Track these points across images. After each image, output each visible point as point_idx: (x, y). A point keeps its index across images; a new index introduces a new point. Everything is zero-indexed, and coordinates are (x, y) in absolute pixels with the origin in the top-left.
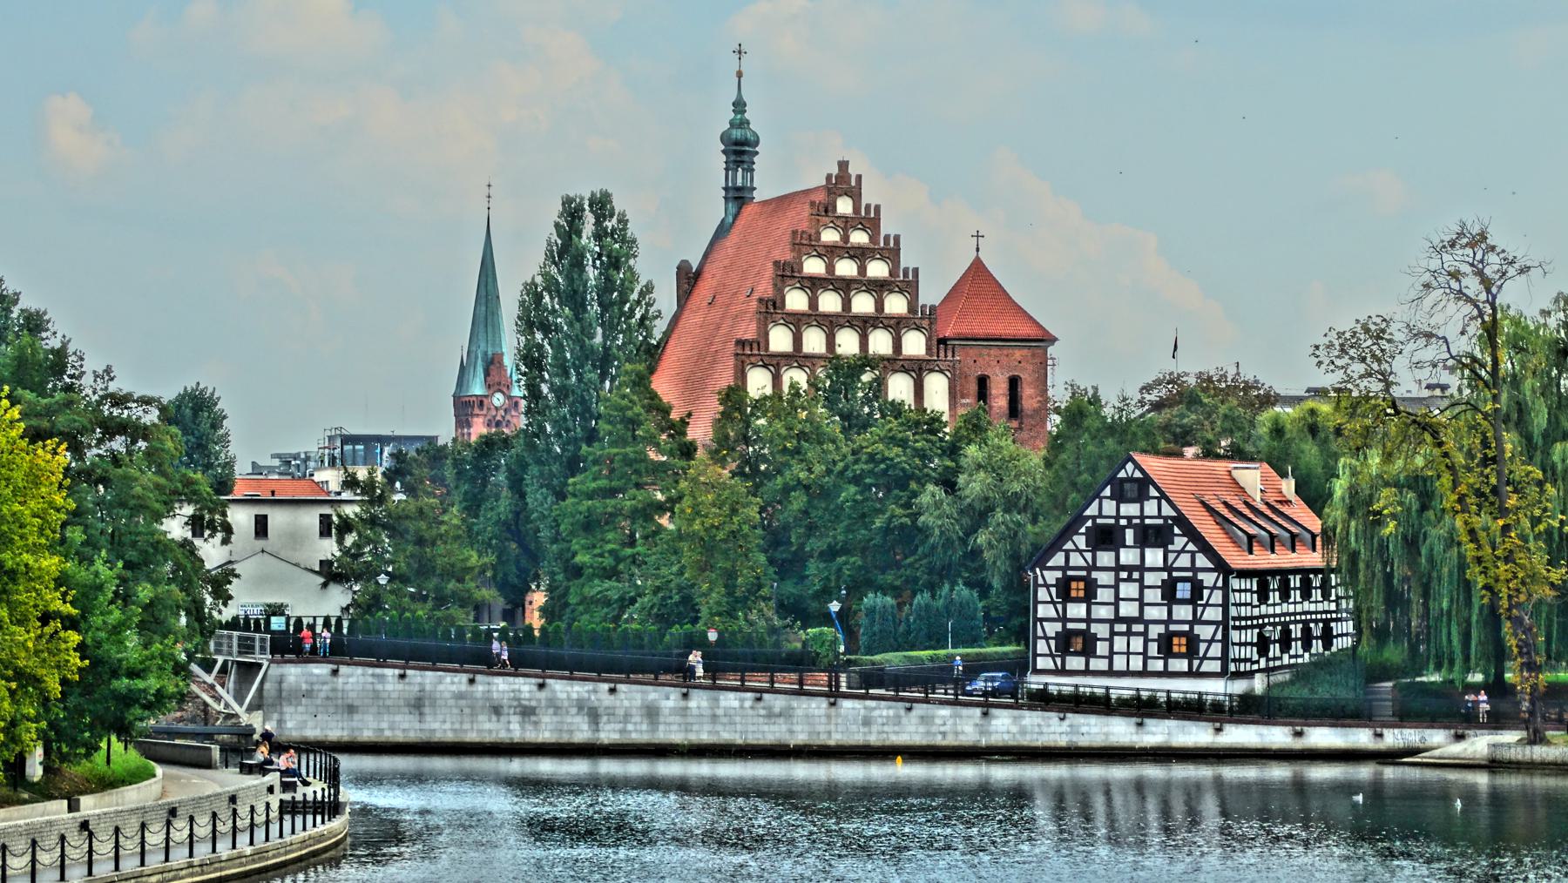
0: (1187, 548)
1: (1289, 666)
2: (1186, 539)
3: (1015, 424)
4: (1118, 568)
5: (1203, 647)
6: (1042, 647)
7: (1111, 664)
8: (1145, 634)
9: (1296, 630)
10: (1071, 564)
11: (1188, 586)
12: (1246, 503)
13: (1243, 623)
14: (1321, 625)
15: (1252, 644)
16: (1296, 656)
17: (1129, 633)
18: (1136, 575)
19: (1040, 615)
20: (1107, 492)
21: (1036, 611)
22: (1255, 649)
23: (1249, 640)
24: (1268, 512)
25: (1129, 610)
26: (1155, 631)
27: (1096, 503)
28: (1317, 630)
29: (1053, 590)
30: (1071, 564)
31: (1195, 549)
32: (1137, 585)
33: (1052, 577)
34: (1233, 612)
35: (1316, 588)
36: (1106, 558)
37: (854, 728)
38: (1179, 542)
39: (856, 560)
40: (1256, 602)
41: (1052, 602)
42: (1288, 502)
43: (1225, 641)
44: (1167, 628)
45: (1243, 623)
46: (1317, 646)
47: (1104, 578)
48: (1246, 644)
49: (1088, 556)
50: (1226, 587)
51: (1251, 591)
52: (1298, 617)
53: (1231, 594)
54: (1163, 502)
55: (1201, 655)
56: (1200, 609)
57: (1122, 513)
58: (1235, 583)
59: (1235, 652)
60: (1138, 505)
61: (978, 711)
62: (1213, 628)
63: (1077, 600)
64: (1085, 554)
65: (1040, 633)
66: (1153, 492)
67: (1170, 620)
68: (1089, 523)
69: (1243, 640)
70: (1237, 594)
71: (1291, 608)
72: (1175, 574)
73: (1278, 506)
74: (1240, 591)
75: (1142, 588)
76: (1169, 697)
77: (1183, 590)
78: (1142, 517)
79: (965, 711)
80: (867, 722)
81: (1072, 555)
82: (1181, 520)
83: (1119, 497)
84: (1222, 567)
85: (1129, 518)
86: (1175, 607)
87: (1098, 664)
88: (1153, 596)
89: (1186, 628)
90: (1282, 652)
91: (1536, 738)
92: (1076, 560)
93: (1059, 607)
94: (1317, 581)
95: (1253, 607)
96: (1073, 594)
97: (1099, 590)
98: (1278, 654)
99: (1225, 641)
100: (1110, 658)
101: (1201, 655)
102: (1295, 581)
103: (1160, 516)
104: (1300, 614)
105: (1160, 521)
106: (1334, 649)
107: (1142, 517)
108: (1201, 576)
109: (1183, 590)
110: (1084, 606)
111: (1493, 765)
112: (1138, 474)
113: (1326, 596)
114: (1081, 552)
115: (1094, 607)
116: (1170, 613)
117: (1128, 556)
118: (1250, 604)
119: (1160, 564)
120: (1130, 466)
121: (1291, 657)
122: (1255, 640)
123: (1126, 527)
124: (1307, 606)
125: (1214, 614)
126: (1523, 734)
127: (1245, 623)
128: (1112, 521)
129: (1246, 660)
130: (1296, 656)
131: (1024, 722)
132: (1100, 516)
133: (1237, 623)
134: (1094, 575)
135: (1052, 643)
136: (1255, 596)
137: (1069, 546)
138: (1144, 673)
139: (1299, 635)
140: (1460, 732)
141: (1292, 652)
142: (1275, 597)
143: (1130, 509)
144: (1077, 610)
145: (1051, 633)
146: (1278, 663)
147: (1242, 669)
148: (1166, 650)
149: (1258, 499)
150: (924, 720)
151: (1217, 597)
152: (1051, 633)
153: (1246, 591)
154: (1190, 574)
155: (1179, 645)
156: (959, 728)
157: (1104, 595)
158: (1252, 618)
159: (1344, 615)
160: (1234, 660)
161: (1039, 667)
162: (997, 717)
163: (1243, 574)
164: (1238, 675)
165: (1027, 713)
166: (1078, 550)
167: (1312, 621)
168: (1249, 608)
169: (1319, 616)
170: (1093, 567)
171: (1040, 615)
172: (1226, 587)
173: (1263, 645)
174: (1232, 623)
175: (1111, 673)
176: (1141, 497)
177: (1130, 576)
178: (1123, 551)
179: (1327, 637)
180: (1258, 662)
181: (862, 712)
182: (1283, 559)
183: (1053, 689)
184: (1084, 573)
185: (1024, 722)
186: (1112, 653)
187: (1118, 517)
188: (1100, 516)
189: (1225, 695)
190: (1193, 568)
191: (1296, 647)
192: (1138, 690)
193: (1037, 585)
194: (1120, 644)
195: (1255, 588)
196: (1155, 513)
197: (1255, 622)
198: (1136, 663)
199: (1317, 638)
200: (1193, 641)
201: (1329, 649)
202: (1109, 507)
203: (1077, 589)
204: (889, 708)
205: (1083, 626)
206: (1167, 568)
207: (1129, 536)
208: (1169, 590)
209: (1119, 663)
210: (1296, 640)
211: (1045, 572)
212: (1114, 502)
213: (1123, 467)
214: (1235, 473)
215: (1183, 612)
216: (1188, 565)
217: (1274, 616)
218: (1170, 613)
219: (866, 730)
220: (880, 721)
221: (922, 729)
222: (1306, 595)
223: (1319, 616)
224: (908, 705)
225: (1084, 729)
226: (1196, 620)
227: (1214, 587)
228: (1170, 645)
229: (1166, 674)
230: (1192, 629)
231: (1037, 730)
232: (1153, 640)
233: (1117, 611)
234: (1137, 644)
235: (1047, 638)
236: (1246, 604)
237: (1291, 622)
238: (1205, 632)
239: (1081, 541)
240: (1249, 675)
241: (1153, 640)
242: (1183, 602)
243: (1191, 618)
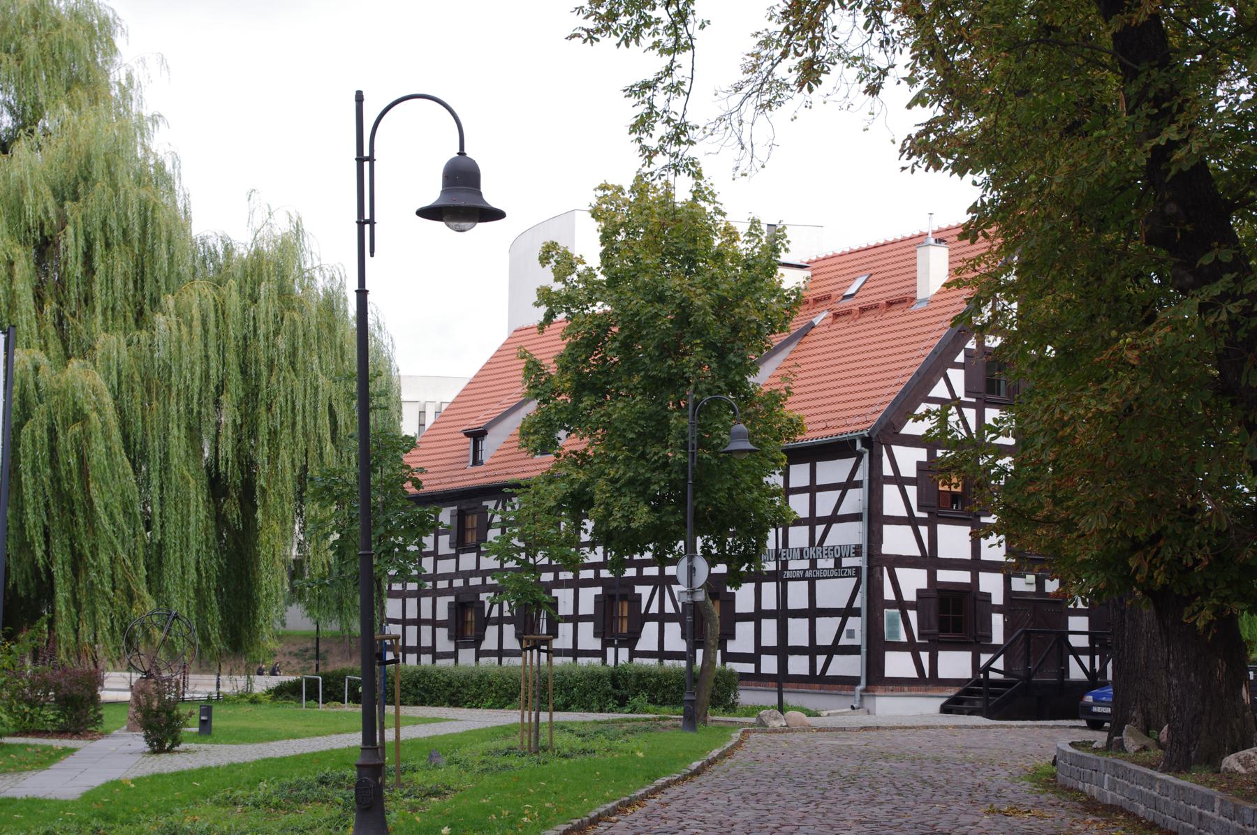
19: (887, 549)
21: (875, 537)
29: (912, 491)
33: (909, 459)
65: (889, 594)
93: (924, 530)
135: (913, 615)
137: (940, 390)
145: (909, 595)
152: (909, 595)
161: (889, 673)
166: (955, 401)
171: (887, 549)
205: (964, 577)
235: (900, 604)
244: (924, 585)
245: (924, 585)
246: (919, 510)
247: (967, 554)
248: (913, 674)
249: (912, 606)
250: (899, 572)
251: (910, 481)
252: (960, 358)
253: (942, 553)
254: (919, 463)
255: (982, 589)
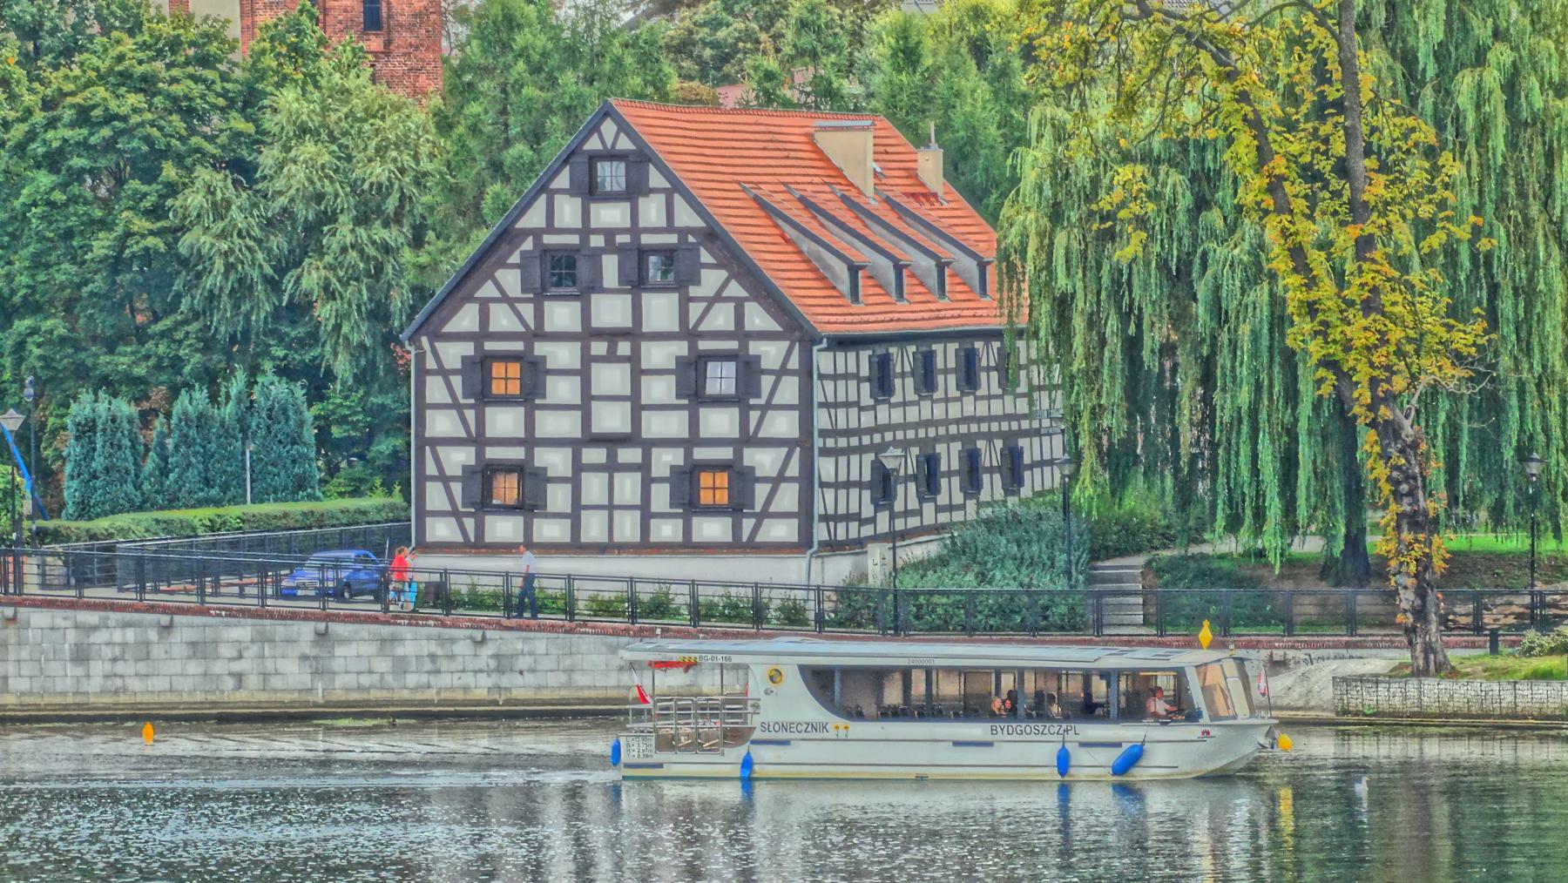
0: (725, 294)
1: (938, 528)
2: (724, 274)
3: (375, 43)
4: (589, 334)
5: (761, 491)
6: (435, 497)
7: (576, 529)
8: (644, 467)
9: (950, 457)
10: (492, 328)
11: (730, 368)
12: (845, 199)
13: (842, 442)
14: (999, 444)
15: (859, 485)
16: (951, 508)
17: (611, 467)
18: (624, 348)
19: (427, 435)
20: (563, 180)
22: (867, 494)
23: (854, 477)
24: (891, 218)
25: (612, 419)
26: (666, 460)
27: (541, 202)
28: (991, 455)
29: (457, 381)
30: (492, 328)
31: (744, 294)
32: (627, 367)
33: (454, 354)
34: (822, 419)
35: (988, 369)
36: (562, 315)
37: (54, 668)
38: (711, 280)
39: (55, 325)
40: (867, 400)
41: (455, 405)
42: (930, 196)
43: (807, 478)
44: (688, 455)
45: (842, 442)
46: (992, 486)
47: (563, 355)
48: (848, 485)
49: (527, 310)
50: (807, 373)
51: (857, 377)
52: (953, 429)
53: (817, 383)
54: (677, 198)
55: (758, 508)
56: (754, 416)
57: (593, 225)
58: (824, 361)
59: (825, 501)
60: (627, 206)
61: (307, 630)
62: (785, 450)
63: (505, 401)
64: (518, 305)
65: (431, 469)
66: (656, 179)
67: (693, 440)
68: (528, 245)
69: (842, 478)
70: (829, 385)
71: (939, 411)
72: (703, 345)
73: (912, 205)
74: (835, 377)
75: (637, 373)
76: (693, 595)
77: (721, 378)
78: (635, 230)
79: (280, 629)
80: (81, 656)
81: (492, 306)
82: (712, 235)
83: (590, 191)
84: (796, 329)
85: (610, 233)
86: (703, 412)
87: (551, 530)
88: (659, 389)
89: (726, 453)
90: (921, 500)
91: (1433, 666)
92: (502, 319)
93: (470, 415)
94: (988, 354)
95: (861, 409)
96: (497, 388)
97: (550, 380)
98: (913, 503)
99: (807, 478)
100: (574, 517)
101: (758, 508)
102: (946, 355)
103: (670, 228)
104: (957, 422)
105: (672, 239)
106: (1026, 492)
107: (635, 230)
108: (755, 348)
109: (721, 378)
110: (521, 410)
111: (1344, 722)
112: (625, 144)
113: (1008, 382)
114: (511, 302)
115: (538, 413)
116: (694, 423)
117: (611, 310)
118: (857, 404)
119: (676, 329)
120: (609, 128)
121: (939, 509)
122: (867, 477)
123: (602, 251)
124: (969, 406)
125: (783, 425)
126: (1406, 656)
127: (845, 443)
128: (574, 240)
129: (848, 518)
130: (951, 508)
131: (400, 651)
132: (550, 228)
133: (830, 443)
134: (541, 348)
136: (866, 387)
137: (488, 290)
138: (645, 547)
139: (955, 466)
140: (1278, 655)
141: (942, 499)
142: (905, 388)
143: (610, 215)
144: (504, 421)
145: (453, 470)
146: (913, 522)
147: (841, 536)
148: (688, 503)
149: (870, 192)
150: (197, 649)
151: (789, 390)
152: (453, 470)
153: (846, 376)
154: (733, 345)
155: (713, 488)
156: (269, 666)
157: (563, 389)
158: (858, 432)
159: (1046, 423)
160: (825, 518)
161: (429, 538)
162: (344, 641)
163: (842, 343)
164: (833, 547)
165: (405, 631)
166: (505, 298)
167: (980, 435)
168: (854, 411)
169: (995, 427)
170: (539, 334)
171: (427, 435)
172: (807, 373)
173: (883, 485)
174: (818, 442)
175: (576, 547)
176: (634, 192)
177: (612, 349)
178: (594, 297)
179: (1013, 468)
180: (873, 520)
181: (72, 636)
182: (913, 313)
183: (460, 585)
184: (518, 346)
185: (400, 651)
186: (577, 505)
187: (586, 231)
188: (550, 228)
189: (808, 588)
190: (742, 334)
191: (950, 490)
192: (631, 580)
193: (423, 372)
194: (594, 487)
195: (865, 371)
196: (663, 224)
197: (866, 440)
198: (627, 527)
199: (991, 470)
200: (741, 478)
201: (1016, 493)
202: (568, 211)
203: (506, 379)
204: (126, 625)
205: (517, 453)
206: (689, 334)
207: (610, 264)
208: (691, 374)
209: (594, 527)
210: (949, 474)
211: (439, 345)
212: (578, 201)
213: (594, 128)
214: (824, 140)
215: (719, 422)
216: (732, 327)
217: (904, 426)
218: (694, 423)
219: (79, 671)
220: (107, 652)
221: (194, 667)
222: (969, 376)
223: (995, 427)
224: (165, 619)
225: (524, 663)
226: (748, 439)
227: (783, 371)
228: (695, 488)
229: (689, 546)
230: (739, 455)
231: (428, 666)
232: (661, 480)
233: (586, 421)
234: (628, 487)
235: (444, 479)
236: (847, 405)
237: (937, 439)
238: (763, 461)
239: (510, 279)
240: (857, 546)
241: (661, 480)
242: (720, 401)
243: (736, 435)
244: (472, 462)
245: (472, 462)
246: (465, 396)
247: (521, 434)
248: (460, 539)
249: (455, 479)
250: (440, 449)
251: (455, 372)
252: (515, 258)
253: (490, 433)
254: (464, 359)
255: (537, 463)
